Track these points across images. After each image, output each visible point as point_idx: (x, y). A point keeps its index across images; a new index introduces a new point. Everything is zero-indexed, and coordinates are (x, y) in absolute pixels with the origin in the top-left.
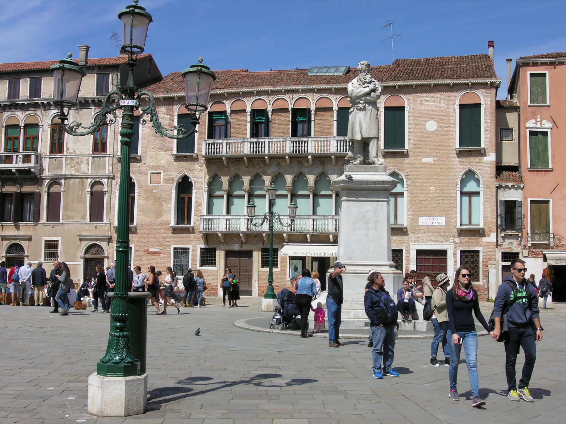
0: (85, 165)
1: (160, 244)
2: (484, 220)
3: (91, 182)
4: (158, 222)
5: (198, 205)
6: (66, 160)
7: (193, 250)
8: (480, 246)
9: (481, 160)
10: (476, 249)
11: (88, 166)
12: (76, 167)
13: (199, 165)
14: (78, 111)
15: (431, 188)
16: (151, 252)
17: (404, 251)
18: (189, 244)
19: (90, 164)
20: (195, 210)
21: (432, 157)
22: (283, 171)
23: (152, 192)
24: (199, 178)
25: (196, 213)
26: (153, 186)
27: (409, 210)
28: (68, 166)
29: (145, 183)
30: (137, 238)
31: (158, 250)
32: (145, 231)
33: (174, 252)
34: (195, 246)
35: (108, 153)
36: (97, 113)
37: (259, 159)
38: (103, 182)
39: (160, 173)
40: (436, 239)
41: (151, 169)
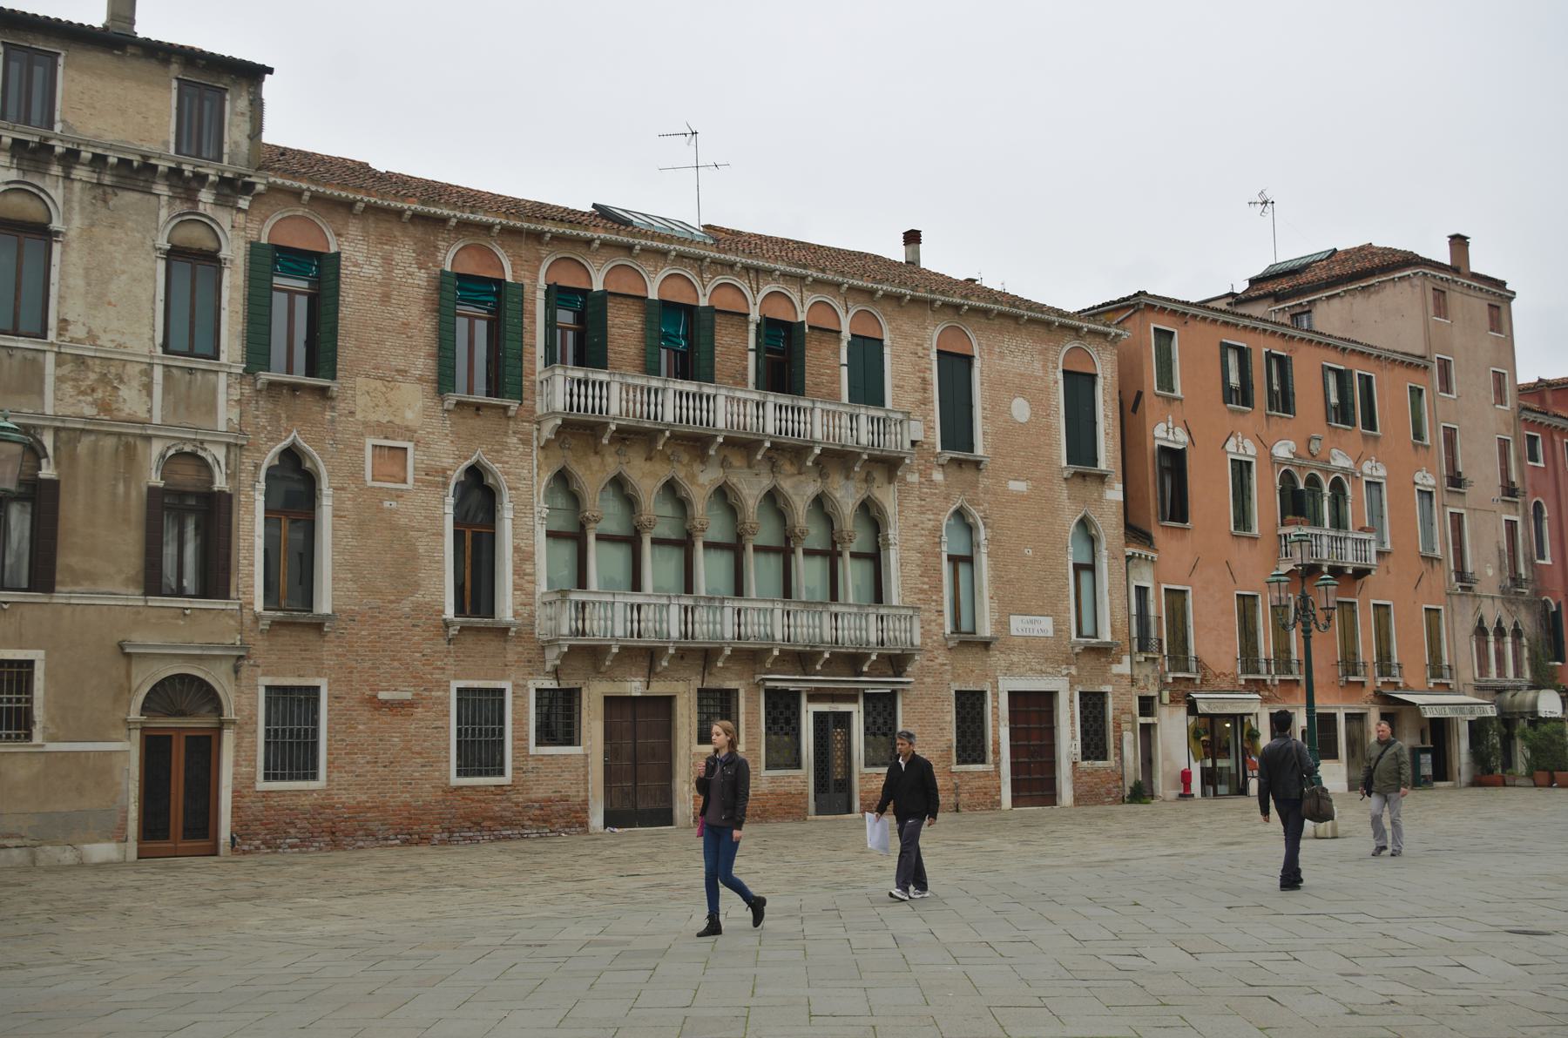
0: (134, 393)
1: (415, 677)
2: (1112, 626)
3: (163, 456)
4: (406, 606)
5: (523, 560)
6: (58, 364)
7: (515, 697)
8: (1105, 682)
9: (1101, 497)
10: (1104, 689)
11: (150, 395)
12: (99, 394)
13: (520, 439)
14: (105, 193)
15: (1026, 550)
16: (385, 703)
17: (989, 694)
18: (502, 678)
19: (158, 391)
20: (515, 572)
21: (1023, 481)
22: (735, 480)
23: (381, 510)
24: (520, 478)
25: (518, 581)
26: (381, 488)
27: (992, 598)
28: (68, 387)
29: (357, 475)
30: (337, 655)
31: (408, 696)
32: (363, 633)
33: (459, 700)
34: (521, 682)
35: (224, 358)
36: (179, 215)
37: (679, 441)
38: (210, 460)
39: (406, 449)
40: (1038, 667)
41: (374, 434)
